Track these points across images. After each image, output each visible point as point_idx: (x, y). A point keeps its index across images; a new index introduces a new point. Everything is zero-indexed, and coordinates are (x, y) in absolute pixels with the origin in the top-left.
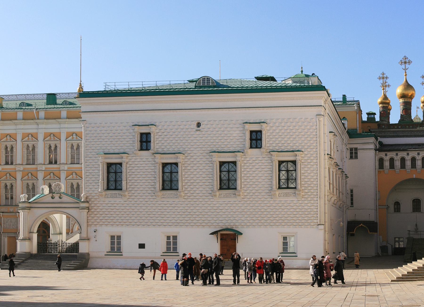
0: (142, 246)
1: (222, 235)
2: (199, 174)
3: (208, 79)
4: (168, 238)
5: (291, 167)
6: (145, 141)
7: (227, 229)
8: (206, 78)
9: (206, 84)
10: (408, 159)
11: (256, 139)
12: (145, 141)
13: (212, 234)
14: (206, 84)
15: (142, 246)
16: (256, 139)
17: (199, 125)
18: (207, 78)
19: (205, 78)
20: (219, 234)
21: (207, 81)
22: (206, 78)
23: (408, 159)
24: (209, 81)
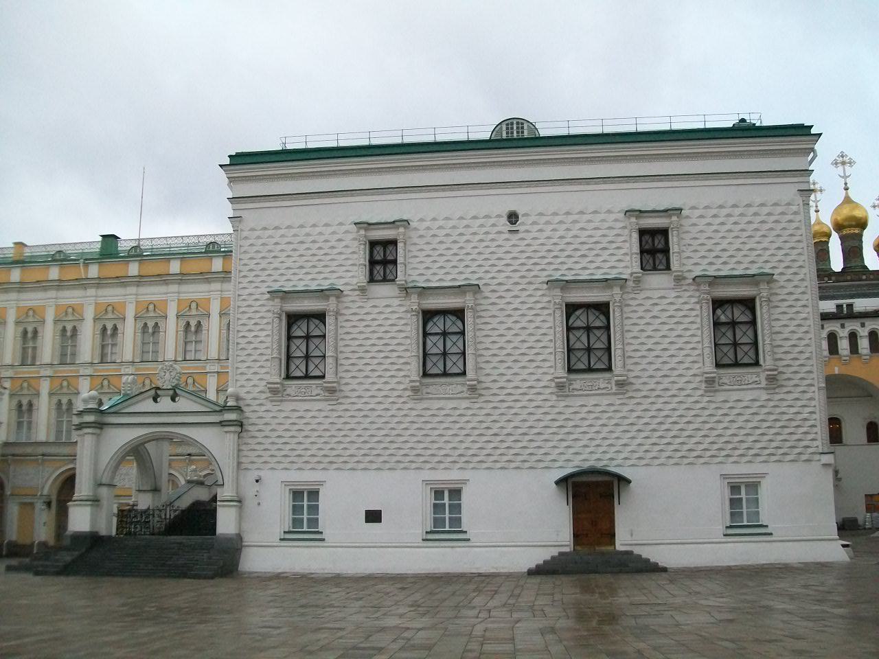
0: (373, 517)
1: (575, 485)
2: (518, 338)
3: (521, 122)
4: (438, 494)
5: (740, 315)
6: (382, 258)
7: (593, 472)
8: (515, 122)
9: (515, 132)
10: (843, 334)
11: (654, 247)
12: (382, 258)
13: (557, 483)
14: (515, 134)
15: (373, 517)
16: (654, 247)
17: (513, 217)
18: (518, 123)
19: (512, 124)
20: (570, 482)
21: (518, 128)
22: (515, 122)
23: (843, 334)
24: (522, 128)
